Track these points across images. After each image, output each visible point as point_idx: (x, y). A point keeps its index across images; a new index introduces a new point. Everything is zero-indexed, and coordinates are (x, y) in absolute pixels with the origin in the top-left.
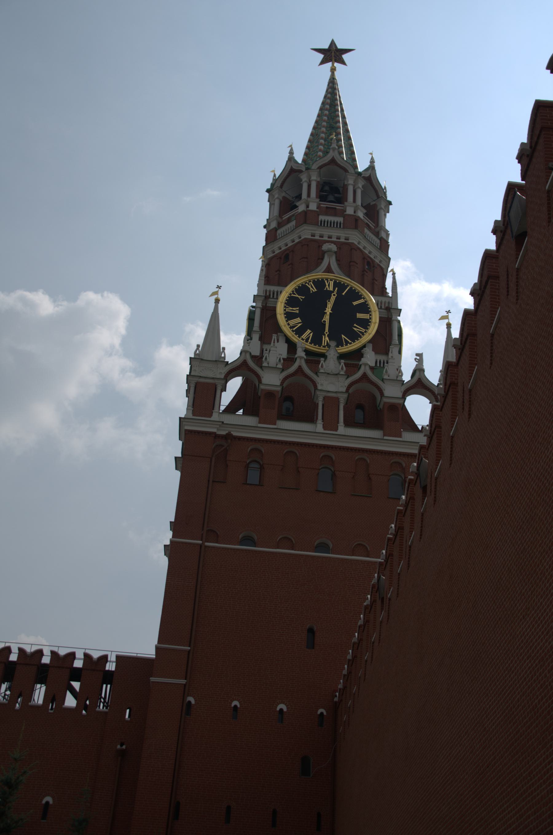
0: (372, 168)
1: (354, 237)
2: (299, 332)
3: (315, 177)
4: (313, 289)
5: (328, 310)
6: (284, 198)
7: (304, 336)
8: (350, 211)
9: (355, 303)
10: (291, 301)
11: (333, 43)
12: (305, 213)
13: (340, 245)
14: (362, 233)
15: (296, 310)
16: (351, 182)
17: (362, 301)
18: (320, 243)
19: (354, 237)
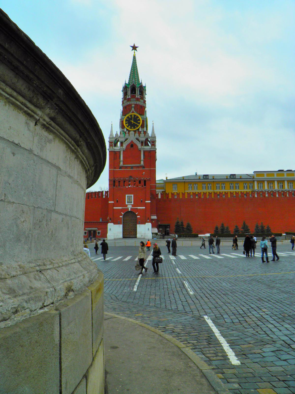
0: (141, 83)
1: (138, 103)
2: (128, 127)
3: (130, 89)
4: (130, 117)
5: (133, 121)
6: (125, 92)
7: (129, 127)
8: (137, 97)
9: (138, 119)
10: (126, 120)
11: (134, 45)
12: (128, 98)
13: (135, 105)
14: (139, 101)
15: (127, 122)
16: (137, 89)
17: (139, 118)
18: (131, 105)
19: (138, 103)
